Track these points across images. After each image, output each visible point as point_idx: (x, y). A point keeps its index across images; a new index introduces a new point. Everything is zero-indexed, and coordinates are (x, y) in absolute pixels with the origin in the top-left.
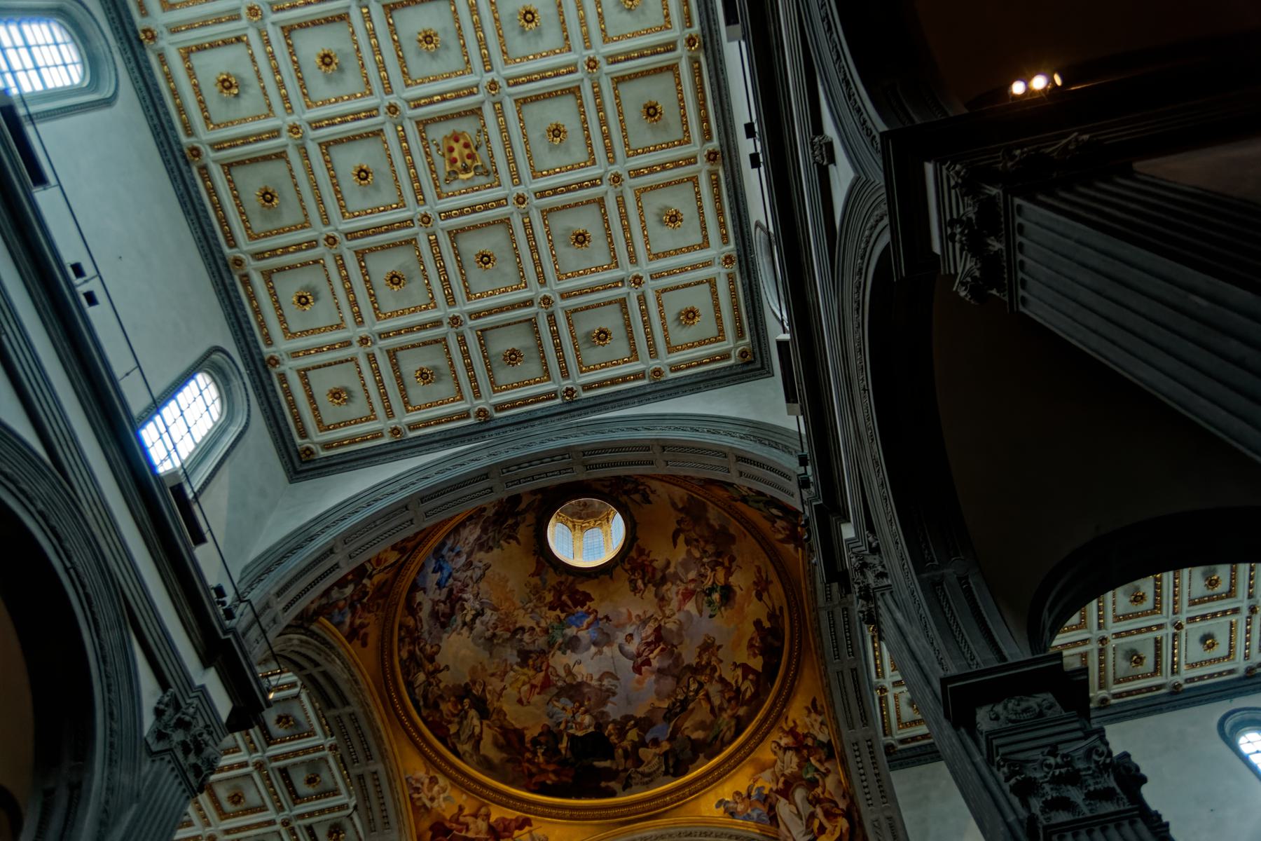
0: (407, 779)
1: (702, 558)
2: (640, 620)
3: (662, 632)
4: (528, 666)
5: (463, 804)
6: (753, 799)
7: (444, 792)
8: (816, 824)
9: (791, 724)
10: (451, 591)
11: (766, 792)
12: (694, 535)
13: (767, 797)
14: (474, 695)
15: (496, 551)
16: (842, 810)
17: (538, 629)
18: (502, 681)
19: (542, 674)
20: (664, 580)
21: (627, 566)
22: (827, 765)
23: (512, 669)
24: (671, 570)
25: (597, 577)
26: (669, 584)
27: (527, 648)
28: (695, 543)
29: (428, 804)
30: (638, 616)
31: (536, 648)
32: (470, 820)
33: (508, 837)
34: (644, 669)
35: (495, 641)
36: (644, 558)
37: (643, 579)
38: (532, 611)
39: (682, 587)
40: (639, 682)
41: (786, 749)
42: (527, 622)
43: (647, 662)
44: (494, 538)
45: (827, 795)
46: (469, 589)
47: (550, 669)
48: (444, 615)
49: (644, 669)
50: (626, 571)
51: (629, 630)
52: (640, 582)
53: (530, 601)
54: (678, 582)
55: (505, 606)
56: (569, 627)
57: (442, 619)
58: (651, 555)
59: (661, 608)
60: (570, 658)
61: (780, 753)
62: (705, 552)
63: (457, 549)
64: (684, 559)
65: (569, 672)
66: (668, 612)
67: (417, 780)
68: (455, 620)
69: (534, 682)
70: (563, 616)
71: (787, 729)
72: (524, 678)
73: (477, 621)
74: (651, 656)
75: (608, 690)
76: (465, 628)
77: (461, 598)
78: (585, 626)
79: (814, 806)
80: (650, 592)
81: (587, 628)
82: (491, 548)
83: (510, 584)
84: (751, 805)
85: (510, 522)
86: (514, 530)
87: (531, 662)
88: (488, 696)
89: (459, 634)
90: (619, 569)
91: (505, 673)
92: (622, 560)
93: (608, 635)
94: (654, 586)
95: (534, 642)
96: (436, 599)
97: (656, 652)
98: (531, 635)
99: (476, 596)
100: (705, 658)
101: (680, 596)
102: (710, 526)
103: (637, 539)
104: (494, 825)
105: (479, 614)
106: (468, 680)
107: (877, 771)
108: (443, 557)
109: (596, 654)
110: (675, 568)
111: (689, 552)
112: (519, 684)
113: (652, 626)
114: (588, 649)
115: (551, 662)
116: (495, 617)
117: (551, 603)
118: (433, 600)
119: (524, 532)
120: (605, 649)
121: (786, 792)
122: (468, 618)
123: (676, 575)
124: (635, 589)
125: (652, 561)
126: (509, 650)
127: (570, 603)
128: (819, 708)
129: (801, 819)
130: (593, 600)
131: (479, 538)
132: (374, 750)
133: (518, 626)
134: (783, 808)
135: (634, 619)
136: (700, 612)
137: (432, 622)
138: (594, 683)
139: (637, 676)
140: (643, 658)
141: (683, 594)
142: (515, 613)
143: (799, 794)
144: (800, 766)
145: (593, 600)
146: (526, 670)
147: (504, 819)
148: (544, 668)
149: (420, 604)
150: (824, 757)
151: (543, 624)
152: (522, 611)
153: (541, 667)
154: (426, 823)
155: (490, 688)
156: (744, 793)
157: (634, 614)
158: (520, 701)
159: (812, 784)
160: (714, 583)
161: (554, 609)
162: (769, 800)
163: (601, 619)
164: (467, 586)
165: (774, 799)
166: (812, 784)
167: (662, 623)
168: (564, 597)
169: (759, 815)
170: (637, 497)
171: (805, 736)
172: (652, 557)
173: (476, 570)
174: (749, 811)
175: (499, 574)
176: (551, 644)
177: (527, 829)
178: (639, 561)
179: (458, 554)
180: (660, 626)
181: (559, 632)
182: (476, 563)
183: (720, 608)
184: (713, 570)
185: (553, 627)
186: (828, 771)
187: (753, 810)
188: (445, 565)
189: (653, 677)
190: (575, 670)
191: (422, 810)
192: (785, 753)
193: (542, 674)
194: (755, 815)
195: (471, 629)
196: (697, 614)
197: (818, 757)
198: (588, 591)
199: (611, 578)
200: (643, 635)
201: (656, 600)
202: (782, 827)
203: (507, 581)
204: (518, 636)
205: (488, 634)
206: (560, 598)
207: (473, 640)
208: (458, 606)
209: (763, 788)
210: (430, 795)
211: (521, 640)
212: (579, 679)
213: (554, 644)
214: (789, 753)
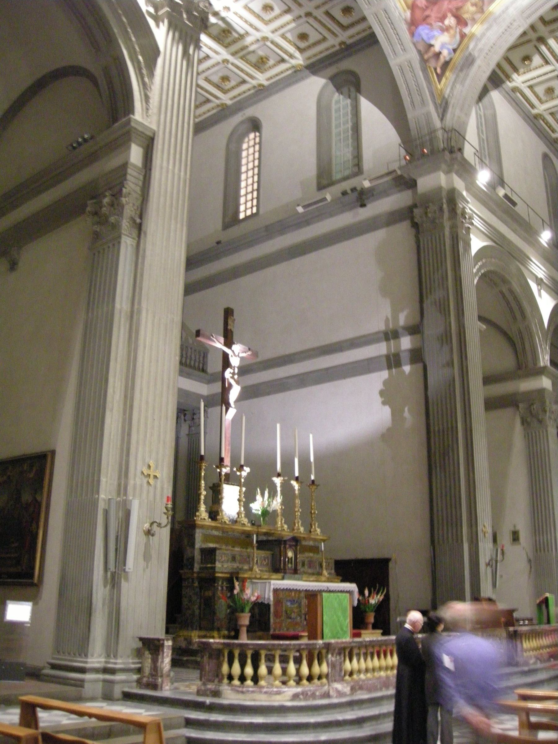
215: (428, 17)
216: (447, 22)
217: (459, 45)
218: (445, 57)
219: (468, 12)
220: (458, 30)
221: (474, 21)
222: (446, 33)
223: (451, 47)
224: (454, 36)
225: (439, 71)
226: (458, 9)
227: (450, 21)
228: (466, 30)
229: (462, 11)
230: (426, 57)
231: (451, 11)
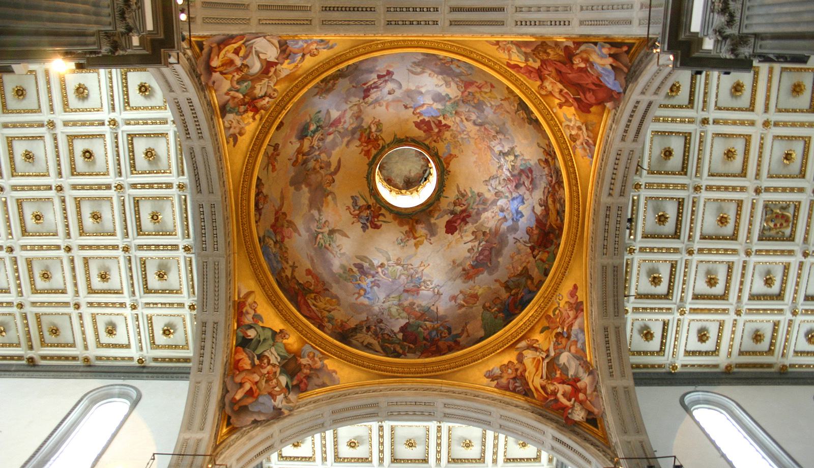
0: (592, 157)
1: (319, 155)
2: (379, 103)
3: (362, 95)
4: (478, 100)
5: (558, 107)
6: (301, 54)
7: (568, 126)
8: (242, 54)
9: (258, 117)
10: (517, 187)
11: (287, 62)
12: (322, 171)
13: (287, 58)
14: (526, 114)
15: (476, 192)
16: (216, 72)
17: (463, 117)
18: (501, 104)
19: (469, 90)
20: (353, 132)
21: (381, 142)
22: (228, 97)
23: (492, 106)
24: (346, 140)
25: (407, 138)
26: (350, 129)
27: (474, 110)
28: (323, 165)
29: (584, 128)
30: (380, 106)
31: (468, 107)
32: (557, 95)
33: (529, 66)
34: (385, 73)
35: (498, 129)
36: (366, 148)
37: (370, 132)
38: (463, 131)
39: (340, 127)
40: (390, 66)
41: (262, 97)
42: (469, 125)
43: (379, 77)
44: (474, 203)
45: (231, 76)
46: (504, 177)
47: (462, 90)
48: (528, 177)
49: (385, 73)
50: (383, 139)
51: (390, 97)
52: (374, 129)
53: (462, 138)
54: (342, 131)
55: (483, 146)
56: (439, 109)
57: (530, 175)
58: (360, 151)
59: (360, 111)
60: (443, 90)
61: (270, 91)
62: (316, 160)
63: (501, 215)
64: (334, 149)
65: (447, 84)
66: (356, 108)
67: (584, 149)
68: (521, 165)
69: (478, 90)
70: (441, 118)
71: (262, 111)
72: (485, 96)
73: (506, 151)
74: (377, 80)
75: (418, 65)
76: (516, 154)
77: (512, 176)
78: (425, 107)
79: (243, 64)
80: (367, 121)
81: (423, 105)
82: (479, 195)
83: (474, 158)
84: (304, 49)
85: (459, 209)
86: (458, 199)
87: (476, 101)
88: (516, 105)
89: (523, 155)
90: (388, 141)
91: (498, 106)
92: (383, 147)
93: (409, 97)
94: (363, 127)
95: (469, 111)
96: (527, 192)
97: (372, 82)
98: (470, 117)
99: (500, 167)
100: (330, 85)
101: (343, 120)
102: (308, 185)
103: (368, 164)
104: (538, 79)
105: (505, 154)
106: (527, 125)
107: (183, 118)
108: (513, 219)
109: (422, 87)
110: (342, 142)
111: (329, 157)
112: (489, 94)
113: (370, 100)
114: (428, 92)
115: (460, 94)
116: (493, 143)
117: (448, 130)
118: (531, 195)
119: (451, 195)
120: (413, 88)
121: (268, 66)
122: (512, 158)
123: (343, 137)
124: (379, 124)
125: (360, 146)
126: (490, 116)
127: (433, 125)
128: (231, 140)
129: (256, 51)
130: (414, 122)
131: (485, 210)
132: (602, 213)
133: (478, 128)
134: (271, 53)
135: (384, 104)
136: (328, 112)
137: (538, 182)
138: (429, 72)
139: (391, 70)
140: (383, 79)
141: (340, 123)
142: (476, 137)
143: (256, 67)
144: (254, 88)
145: (414, 122)
146: (481, 99)
147: (529, 77)
148: (466, 93)
149: (541, 206)
150: (230, 102)
151: (458, 119)
152: (472, 134)
153: (469, 94)
154: (591, 118)
155: (513, 108)
156: (308, 57)
157: (384, 108)
158: (492, 86)
159: (240, 81)
160: (313, 137)
161: (445, 125)
162: (285, 56)
163: (411, 107)
164: (504, 179)
165: (280, 58)
166: (240, 81)
167: (361, 101)
168: (436, 130)
169: (297, 43)
170: (361, 202)
171: (246, 111)
172: (361, 148)
173: (494, 186)
174: (305, 45)
175: (479, 171)
176: (456, 103)
177: (512, 63)
178: (370, 146)
179: (502, 210)
180: (364, 98)
181: (448, 109)
182: (493, 192)
183: (311, 120)
184: (312, 147)
185: (451, 113)
186: (227, 94)
187: (302, 46)
188: (514, 211)
189: (377, 69)
190: (443, 82)
191: (590, 128)
192: (266, 93)
193: (469, 90)
194: (301, 43)
195: (512, 149)
196: (331, 111)
197: (236, 100)
198: (417, 129)
199: (395, 135)
200: (379, 93)
201: (363, 116)
202: (276, 42)
203: (475, 162)
204: (479, 121)
205: (500, 136)
206: (440, 131)
207: (513, 142)
208: (516, 172)
209: (289, 64)
210: (580, 132)
211: (478, 117)
212: (440, 77)
213: (454, 102)
214: (263, 93)
215: (594, 84)
216: (582, 65)
217: (587, 43)
218: (609, 49)
219: (557, 54)
220: (578, 52)
221: (557, 44)
222: (591, 60)
223: (597, 49)
224: (585, 51)
225: (625, 49)
226: (564, 64)
227: (578, 63)
228: (571, 44)
229: (561, 59)
230: (625, 70)
231: (572, 68)
